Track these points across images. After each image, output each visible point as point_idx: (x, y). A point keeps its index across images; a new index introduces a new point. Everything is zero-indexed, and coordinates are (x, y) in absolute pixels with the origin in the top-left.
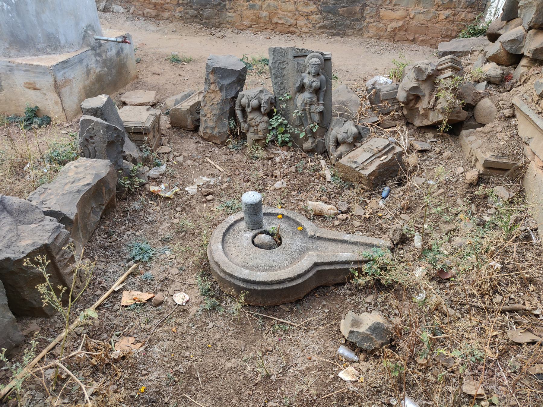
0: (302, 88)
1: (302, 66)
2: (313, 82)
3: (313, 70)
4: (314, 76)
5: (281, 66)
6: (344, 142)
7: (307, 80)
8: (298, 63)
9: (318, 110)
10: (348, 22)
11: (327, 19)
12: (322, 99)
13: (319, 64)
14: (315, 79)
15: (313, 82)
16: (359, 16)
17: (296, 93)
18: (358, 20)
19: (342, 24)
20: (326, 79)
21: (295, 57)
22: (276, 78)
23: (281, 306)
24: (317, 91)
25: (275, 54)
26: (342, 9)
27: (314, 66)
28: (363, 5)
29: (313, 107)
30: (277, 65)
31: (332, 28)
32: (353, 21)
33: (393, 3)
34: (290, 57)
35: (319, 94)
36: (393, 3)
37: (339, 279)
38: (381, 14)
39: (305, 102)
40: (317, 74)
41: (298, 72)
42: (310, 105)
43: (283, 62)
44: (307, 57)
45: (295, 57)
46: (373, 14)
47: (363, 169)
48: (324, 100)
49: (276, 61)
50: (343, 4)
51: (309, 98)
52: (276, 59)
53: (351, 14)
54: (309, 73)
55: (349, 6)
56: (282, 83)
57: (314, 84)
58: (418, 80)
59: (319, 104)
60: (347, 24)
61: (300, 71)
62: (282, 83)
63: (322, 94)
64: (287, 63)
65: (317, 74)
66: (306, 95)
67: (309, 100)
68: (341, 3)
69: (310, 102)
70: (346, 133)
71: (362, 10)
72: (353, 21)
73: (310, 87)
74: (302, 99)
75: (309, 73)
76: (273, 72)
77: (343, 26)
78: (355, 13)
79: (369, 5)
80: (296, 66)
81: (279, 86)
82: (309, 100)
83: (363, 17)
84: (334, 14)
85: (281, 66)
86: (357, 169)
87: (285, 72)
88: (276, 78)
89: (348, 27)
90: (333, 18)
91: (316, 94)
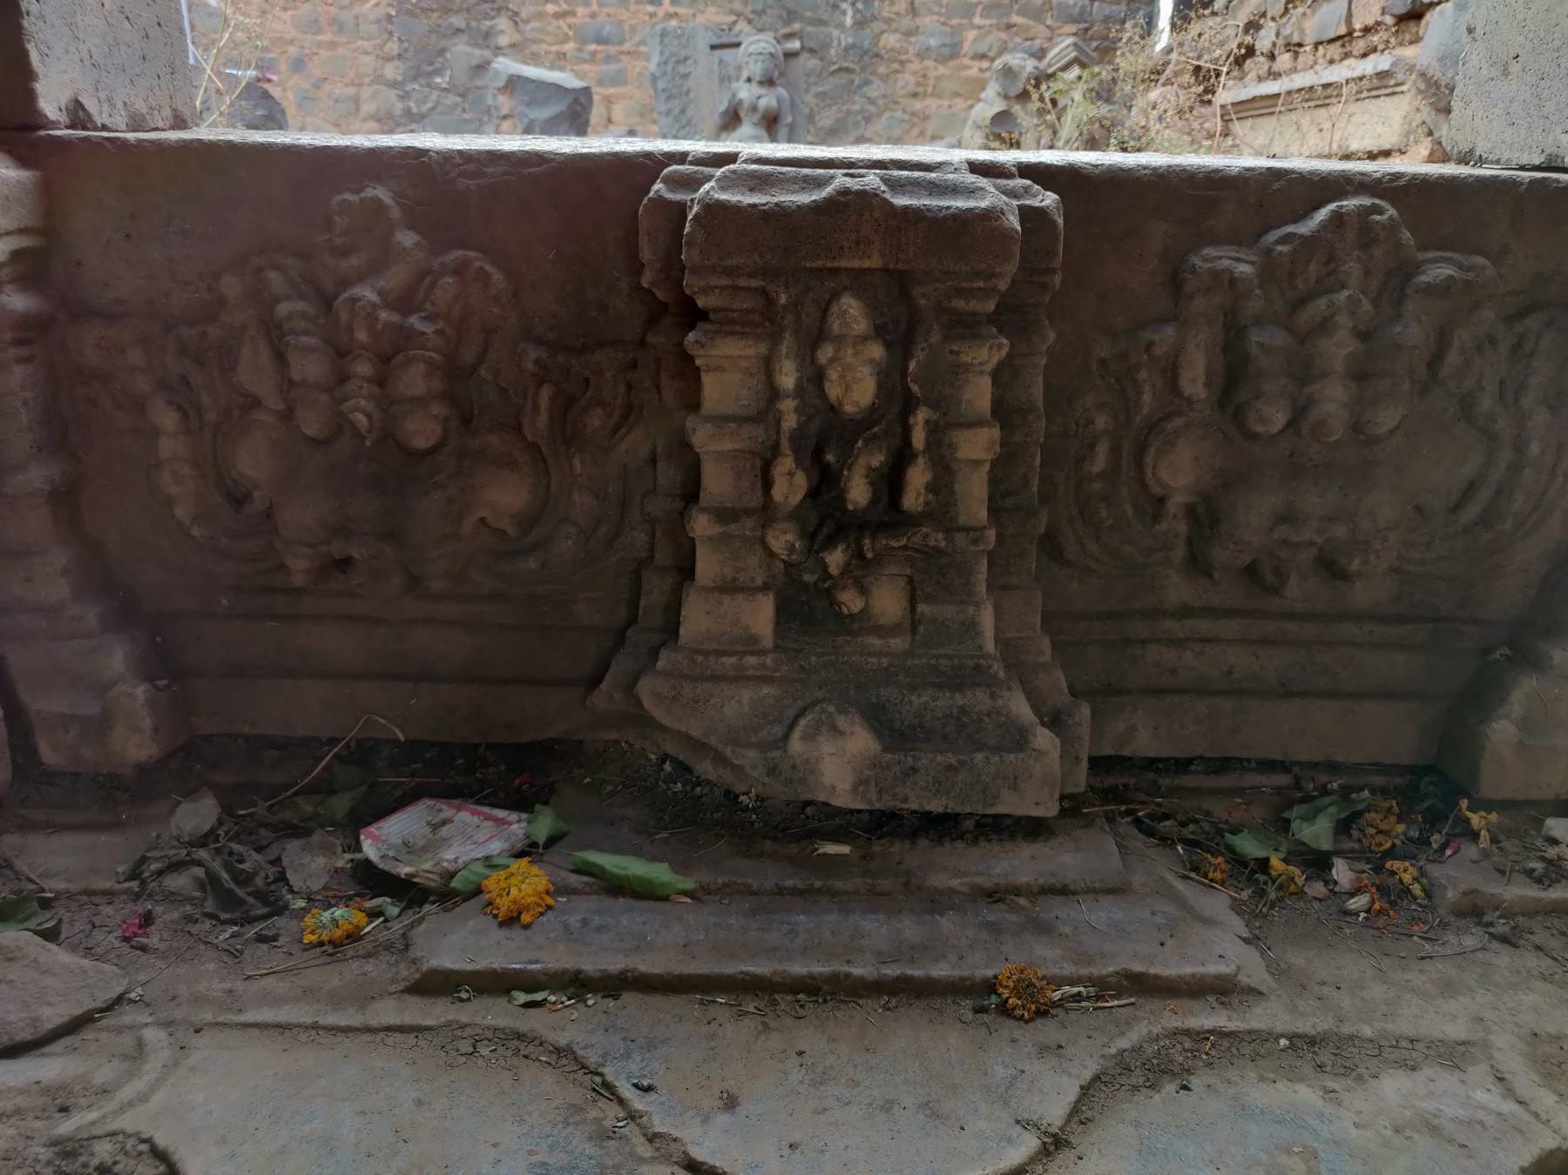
2: (759, 98)
3: (756, 68)
4: (761, 83)
5: (682, 69)
7: (745, 93)
8: (721, 61)
13: (771, 54)
15: (759, 98)
20: (792, 99)
21: (713, 47)
25: (666, 41)
27: (762, 57)
30: (669, 67)
33: (929, 133)
34: (702, 44)
36: (929, 133)
41: (721, 81)
43: (686, 59)
44: (743, 46)
45: (713, 47)
52: (667, 53)
54: (749, 80)
56: (683, 111)
57: (763, 103)
58: (1006, 97)
61: (725, 80)
62: (683, 111)
64: (695, 61)
65: (768, 82)
73: (754, 109)
75: (749, 80)
76: (661, 85)
80: (716, 67)
81: (677, 120)
85: (682, 69)
87: (691, 83)
88: (668, 99)
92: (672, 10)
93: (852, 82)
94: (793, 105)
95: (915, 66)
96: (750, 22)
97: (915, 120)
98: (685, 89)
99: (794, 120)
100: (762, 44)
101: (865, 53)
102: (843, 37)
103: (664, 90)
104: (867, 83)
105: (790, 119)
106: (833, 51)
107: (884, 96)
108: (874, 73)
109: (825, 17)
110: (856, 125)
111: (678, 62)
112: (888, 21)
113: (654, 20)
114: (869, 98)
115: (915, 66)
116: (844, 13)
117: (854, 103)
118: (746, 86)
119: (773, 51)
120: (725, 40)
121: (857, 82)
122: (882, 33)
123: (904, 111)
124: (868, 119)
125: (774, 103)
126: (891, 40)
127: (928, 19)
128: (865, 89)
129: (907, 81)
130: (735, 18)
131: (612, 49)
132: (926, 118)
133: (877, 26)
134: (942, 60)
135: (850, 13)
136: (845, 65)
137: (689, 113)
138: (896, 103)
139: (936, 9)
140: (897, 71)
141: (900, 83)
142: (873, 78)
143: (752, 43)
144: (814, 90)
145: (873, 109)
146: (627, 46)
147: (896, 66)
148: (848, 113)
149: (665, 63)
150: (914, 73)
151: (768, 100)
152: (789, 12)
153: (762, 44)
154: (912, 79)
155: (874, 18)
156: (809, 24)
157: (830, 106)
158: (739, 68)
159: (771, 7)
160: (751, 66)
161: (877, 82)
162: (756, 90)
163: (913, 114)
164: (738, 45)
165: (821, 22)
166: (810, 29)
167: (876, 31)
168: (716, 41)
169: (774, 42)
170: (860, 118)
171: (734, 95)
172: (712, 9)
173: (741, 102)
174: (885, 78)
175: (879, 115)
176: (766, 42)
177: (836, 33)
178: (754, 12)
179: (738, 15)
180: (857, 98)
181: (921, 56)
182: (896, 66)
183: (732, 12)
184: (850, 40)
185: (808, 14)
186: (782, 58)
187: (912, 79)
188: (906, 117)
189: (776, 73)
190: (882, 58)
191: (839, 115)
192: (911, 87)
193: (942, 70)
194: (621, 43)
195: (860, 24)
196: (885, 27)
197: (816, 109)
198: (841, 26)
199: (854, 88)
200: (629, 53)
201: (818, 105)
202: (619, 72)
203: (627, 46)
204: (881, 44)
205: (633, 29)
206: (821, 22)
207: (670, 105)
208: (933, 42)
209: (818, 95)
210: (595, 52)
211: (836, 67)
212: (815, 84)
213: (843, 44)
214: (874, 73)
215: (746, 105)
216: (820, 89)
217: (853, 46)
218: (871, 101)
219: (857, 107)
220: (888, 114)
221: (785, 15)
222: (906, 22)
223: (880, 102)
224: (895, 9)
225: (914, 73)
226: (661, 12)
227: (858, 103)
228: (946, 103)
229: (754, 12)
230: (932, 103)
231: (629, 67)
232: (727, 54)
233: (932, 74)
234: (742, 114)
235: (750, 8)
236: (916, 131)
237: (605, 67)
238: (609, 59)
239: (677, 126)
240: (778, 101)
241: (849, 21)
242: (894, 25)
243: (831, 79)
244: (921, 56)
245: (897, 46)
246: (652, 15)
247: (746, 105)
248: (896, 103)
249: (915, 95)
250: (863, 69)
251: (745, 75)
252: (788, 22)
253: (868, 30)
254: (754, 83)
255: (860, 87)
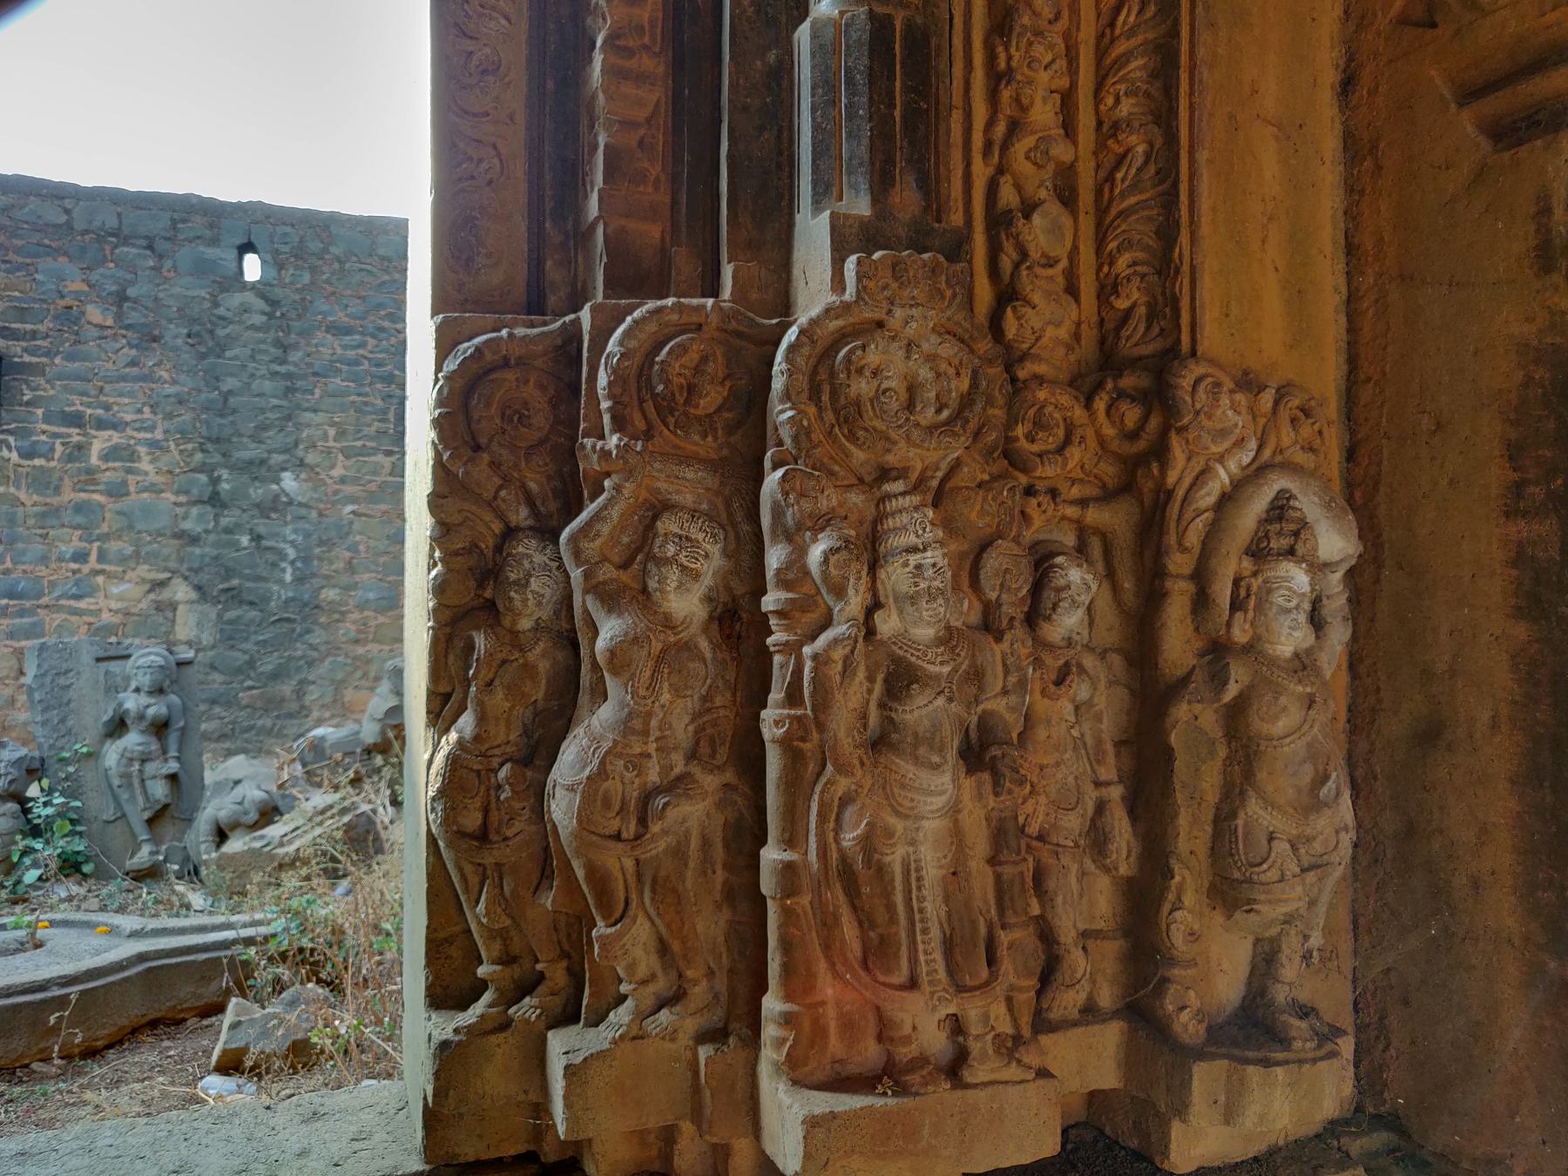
0: (118, 726)
1: (119, 679)
2: (147, 707)
3: (145, 680)
4: (150, 693)
5: (62, 681)
6: (236, 826)
7: (131, 703)
8: (107, 673)
9: (165, 771)
10: (267, 722)
11: (209, 719)
12: (173, 753)
13: (161, 667)
14: (153, 701)
15: (147, 707)
16: (294, 706)
17: (102, 743)
18: (290, 716)
19: (252, 728)
20: (184, 704)
21: (98, 660)
22: (45, 710)
23: (34, 1066)
24: (160, 728)
25: (45, 655)
26: (249, 693)
28: (301, 682)
29: (150, 768)
30: (48, 679)
31: (223, 737)
32: (278, 717)
34: (86, 658)
35: (166, 738)
37: (209, 993)
38: (346, 699)
39: (129, 755)
40: (158, 691)
41: (108, 690)
42: (143, 761)
43: (67, 671)
45: (98, 660)
46: (328, 700)
47: (281, 845)
48: (179, 750)
49: (47, 672)
50: (249, 683)
51: (139, 744)
52: (46, 666)
53: (271, 704)
54: (137, 690)
55: (265, 685)
56: (63, 721)
57: (151, 712)
59: (166, 760)
60: (263, 727)
61: (112, 689)
62: (63, 721)
63: (173, 738)
64: (78, 673)
65: (158, 691)
66: (133, 739)
67: (140, 748)
68: (243, 681)
69: (143, 753)
70: (239, 804)
71: (300, 693)
72: (278, 717)
73: (141, 717)
74: (120, 750)
75: (137, 690)
76: (37, 696)
77: (253, 732)
78: (283, 700)
79: (313, 683)
80: (102, 678)
81: (55, 729)
82: (140, 748)
83: (303, 707)
84: (228, 704)
85: (62, 681)
86: (268, 848)
87: (71, 694)
88: (45, 710)
89: (269, 732)
90: (223, 714)
91: (160, 739)
92: (99, 567)
93: (293, 630)
94: (185, 709)
95: (356, 616)
96: (186, 578)
97: (358, 663)
98: (65, 700)
99: (186, 723)
100: (152, 657)
101: (306, 605)
102: (283, 592)
103: (40, 701)
104: (308, 631)
105: (182, 724)
106: (273, 604)
107: (327, 643)
108: (315, 622)
109: (264, 574)
110: (298, 669)
111: (57, 674)
112: (327, 577)
113: (77, 576)
114: (311, 645)
115: (356, 616)
116: (284, 570)
117: (296, 650)
118: (135, 695)
119: (163, 663)
120: (111, 653)
121: (298, 630)
122: (322, 587)
123: (347, 656)
124: (310, 664)
125: (164, 710)
126: (330, 594)
127: (366, 576)
128: (307, 637)
129: (348, 628)
130: (169, 575)
131: (28, 604)
132: (368, 662)
133: (316, 582)
134: (381, 611)
135: (289, 571)
136: (286, 615)
137: (70, 723)
138: (339, 648)
139: (373, 567)
140: (338, 621)
141: (342, 632)
142: (316, 628)
143: (143, 656)
144: (253, 638)
145: (315, 654)
146: (44, 600)
147: (336, 616)
148: (290, 658)
149: (43, 675)
150: (354, 622)
151: (156, 709)
152: (227, 570)
153: (152, 657)
154: (353, 628)
155: (313, 575)
156: (248, 580)
157: (271, 652)
158: (128, 679)
159: (208, 565)
160: (140, 678)
161: (318, 631)
162: (144, 699)
163: (355, 658)
164: (128, 657)
165: (259, 578)
166: (249, 584)
167: (316, 586)
168: (102, 654)
169: (166, 653)
170: (302, 662)
171: (120, 705)
172: (146, 567)
173: (127, 711)
174: (325, 627)
175: (322, 661)
176: (157, 654)
177: (276, 588)
178: (190, 569)
179: (173, 572)
180: (298, 645)
181: (361, 607)
182: (336, 616)
183: (166, 569)
184: (290, 594)
185: (247, 571)
186: (175, 667)
187: (353, 628)
188: (349, 661)
189: (167, 683)
190: (323, 609)
191: (282, 661)
192: (352, 634)
193: (381, 619)
194: (38, 599)
195: (300, 580)
196: (325, 582)
197: (257, 656)
198: (281, 582)
199: (295, 636)
200: (47, 606)
201: (258, 652)
202: (34, 624)
203: (44, 600)
204: (322, 596)
205: (52, 584)
206: (259, 578)
207: (47, 716)
208: (371, 596)
209: (257, 643)
210: (7, 606)
211: (276, 617)
212: (255, 633)
213: (284, 597)
214: (315, 622)
215: (132, 714)
216: (261, 638)
217: (293, 599)
218: (313, 647)
219: (299, 653)
220: (330, 659)
221: (223, 572)
222: (345, 579)
223: (323, 648)
224: (334, 567)
225: (354, 622)
226: (86, 569)
227: (300, 649)
228: (387, 648)
229: (190, 569)
230: (373, 648)
231: (48, 619)
232: (114, 666)
233: (373, 623)
234: (129, 722)
235: (185, 566)
236: (359, 674)
237: (17, 621)
238: (22, 613)
239: (55, 736)
240: (168, 708)
241: (288, 577)
242: (333, 581)
243: (272, 628)
244: (361, 607)
245: (338, 598)
246: (74, 572)
247: (132, 714)
248: (339, 648)
249: (357, 641)
250: (304, 619)
251: (133, 685)
252: (227, 578)
253: (308, 586)
254: (142, 694)
255: (301, 635)
